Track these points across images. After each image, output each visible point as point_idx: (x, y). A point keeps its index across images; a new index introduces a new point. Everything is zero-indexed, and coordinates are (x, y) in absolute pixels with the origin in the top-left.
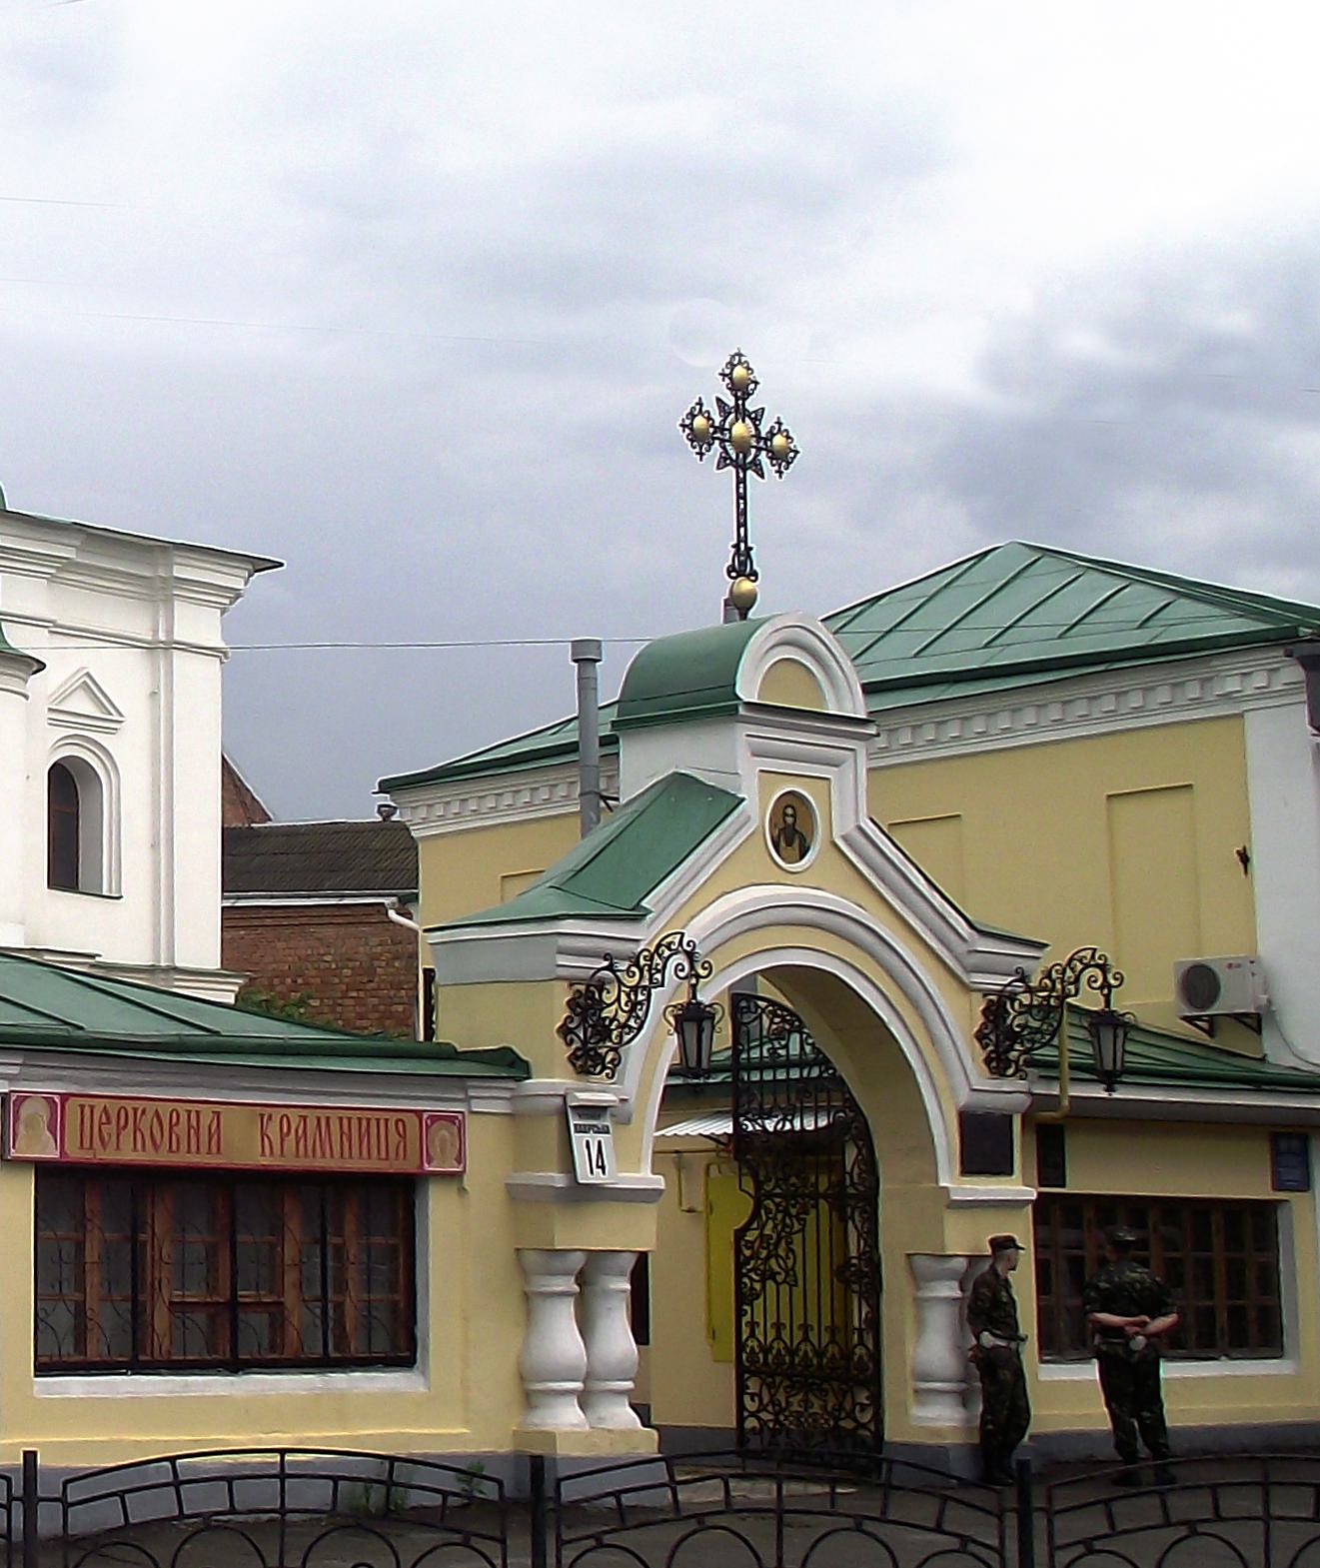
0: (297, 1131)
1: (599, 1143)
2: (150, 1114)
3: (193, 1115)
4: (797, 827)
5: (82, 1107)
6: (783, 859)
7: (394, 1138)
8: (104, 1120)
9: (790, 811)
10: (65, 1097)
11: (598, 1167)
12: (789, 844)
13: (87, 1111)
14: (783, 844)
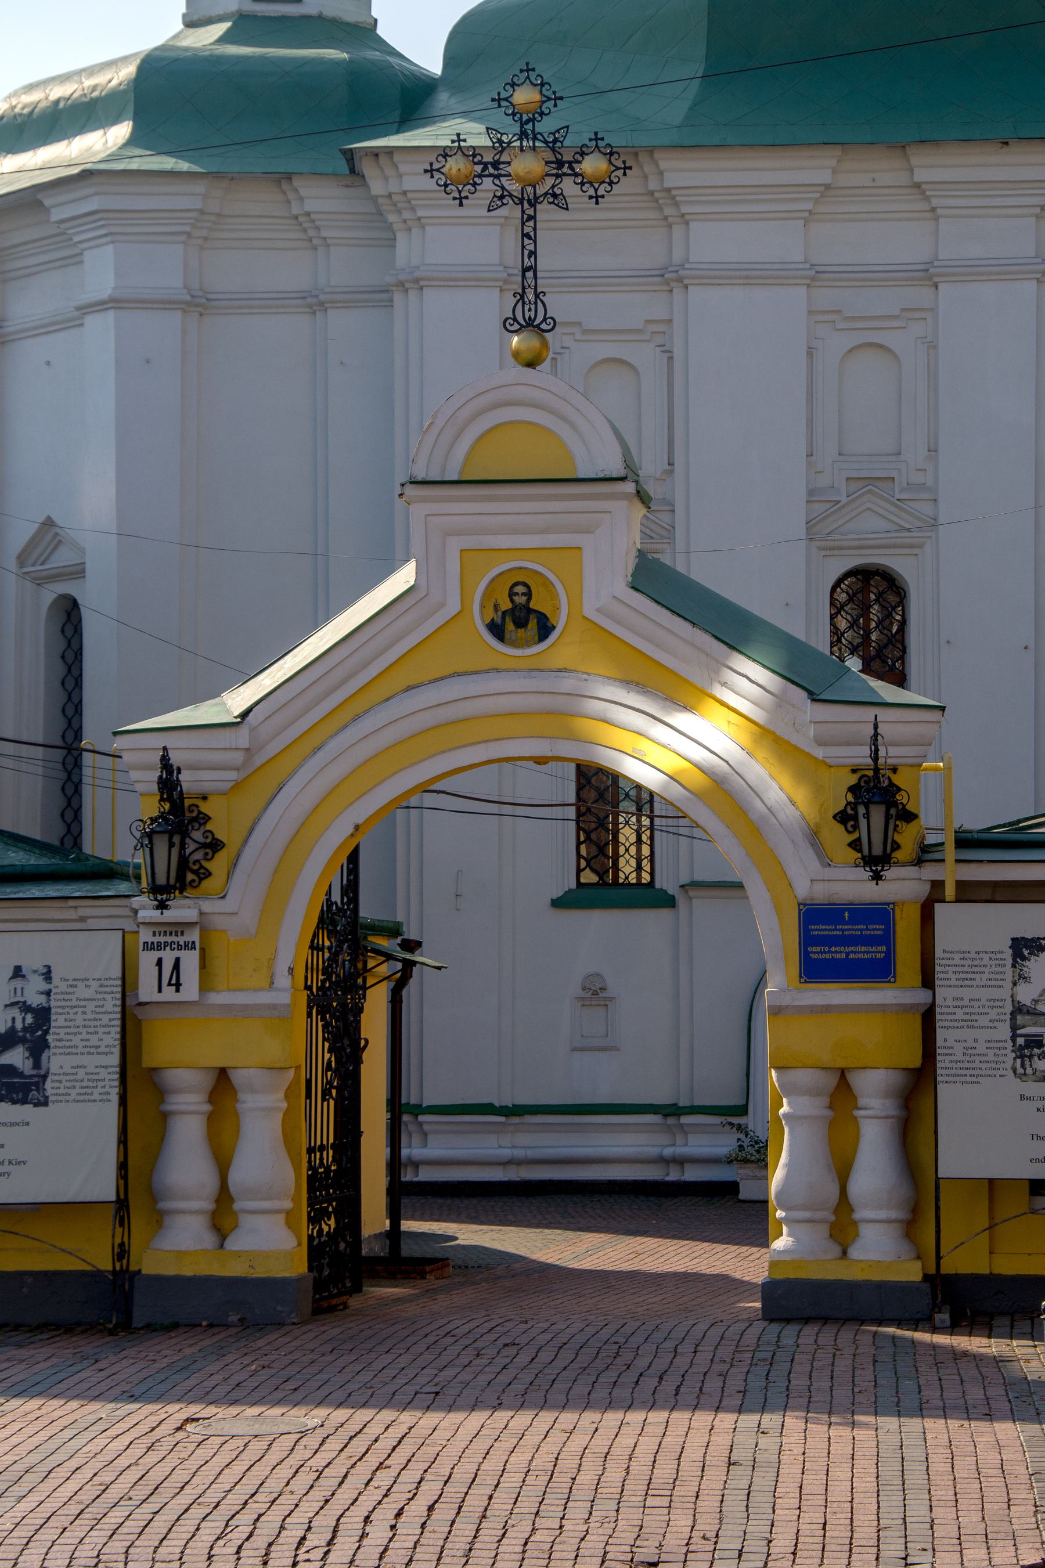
1: (177, 961)
4: (532, 605)
6: (514, 644)
9: (520, 589)
11: (170, 984)
12: (521, 624)
14: (510, 626)
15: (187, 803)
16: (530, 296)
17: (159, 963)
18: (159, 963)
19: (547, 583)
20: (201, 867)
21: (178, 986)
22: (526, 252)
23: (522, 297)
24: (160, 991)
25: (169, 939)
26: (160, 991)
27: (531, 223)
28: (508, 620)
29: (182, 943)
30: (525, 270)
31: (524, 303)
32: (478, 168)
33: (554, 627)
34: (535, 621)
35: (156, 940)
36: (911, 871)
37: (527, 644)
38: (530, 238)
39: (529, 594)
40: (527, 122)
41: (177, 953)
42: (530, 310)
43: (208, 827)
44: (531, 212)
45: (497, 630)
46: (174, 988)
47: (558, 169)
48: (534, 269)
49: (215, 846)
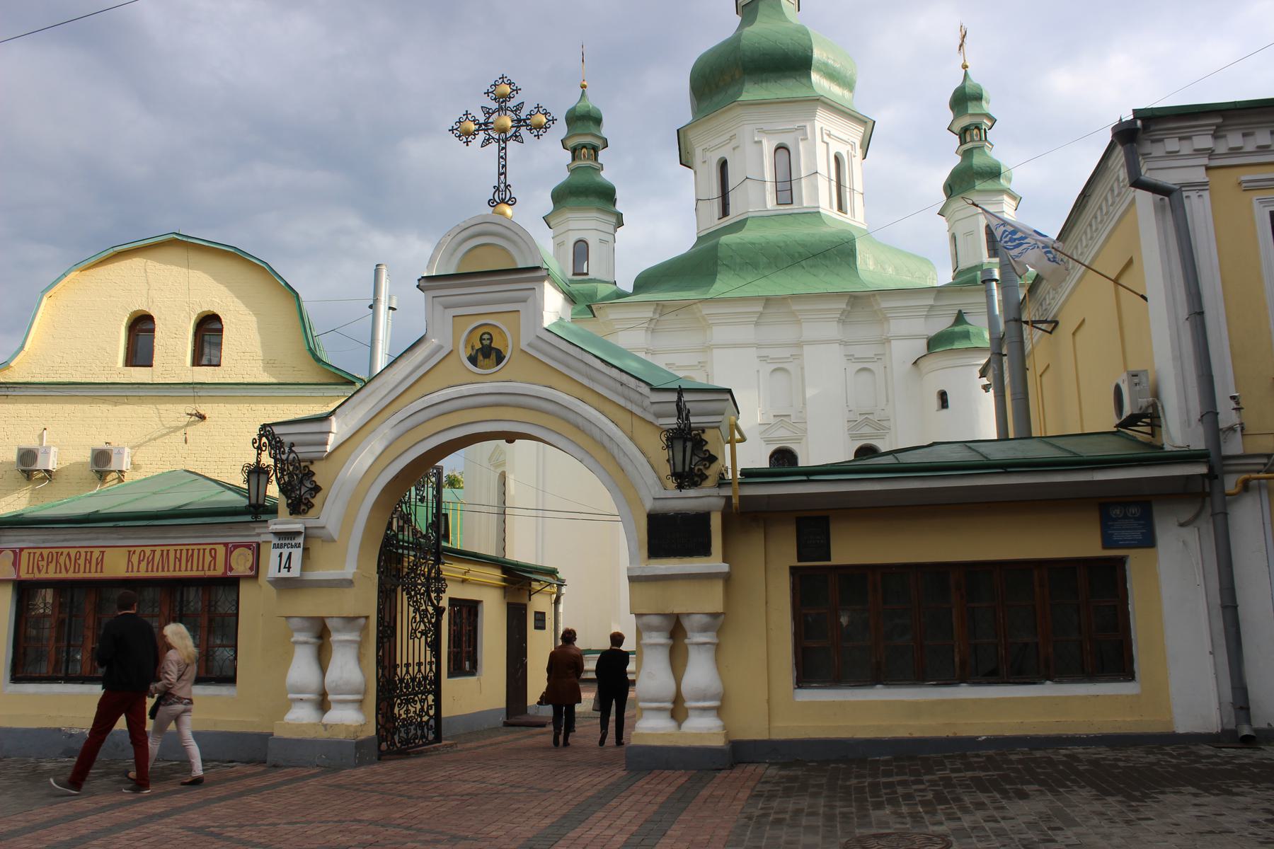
0: (148, 558)
1: (290, 554)
2: (65, 554)
3: (89, 554)
4: (493, 345)
5: (30, 553)
6: (482, 367)
7: (208, 558)
8: (40, 559)
9: (486, 336)
10: (22, 549)
11: (285, 568)
13: (32, 555)
14: (480, 357)
15: (303, 464)
16: (502, 186)
17: (281, 555)
18: (281, 555)
19: (501, 332)
20: (309, 501)
21: (289, 568)
22: (501, 166)
23: (498, 189)
24: (279, 571)
25: (287, 542)
26: (279, 571)
27: (504, 151)
28: (479, 354)
29: (293, 544)
30: (500, 174)
31: (499, 191)
32: (477, 127)
33: (505, 357)
34: (494, 354)
35: (280, 542)
36: (715, 491)
37: (489, 367)
38: (503, 158)
39: (491, 339)
40: (502, 102)
41: (290, 550)
42: (502, 194)
43: (314, 479)
44: (504, 145)
45: (473, 360)
46: (287, 569)
47: (518, 123)
48: (505, 174)
49: (317, 489)
